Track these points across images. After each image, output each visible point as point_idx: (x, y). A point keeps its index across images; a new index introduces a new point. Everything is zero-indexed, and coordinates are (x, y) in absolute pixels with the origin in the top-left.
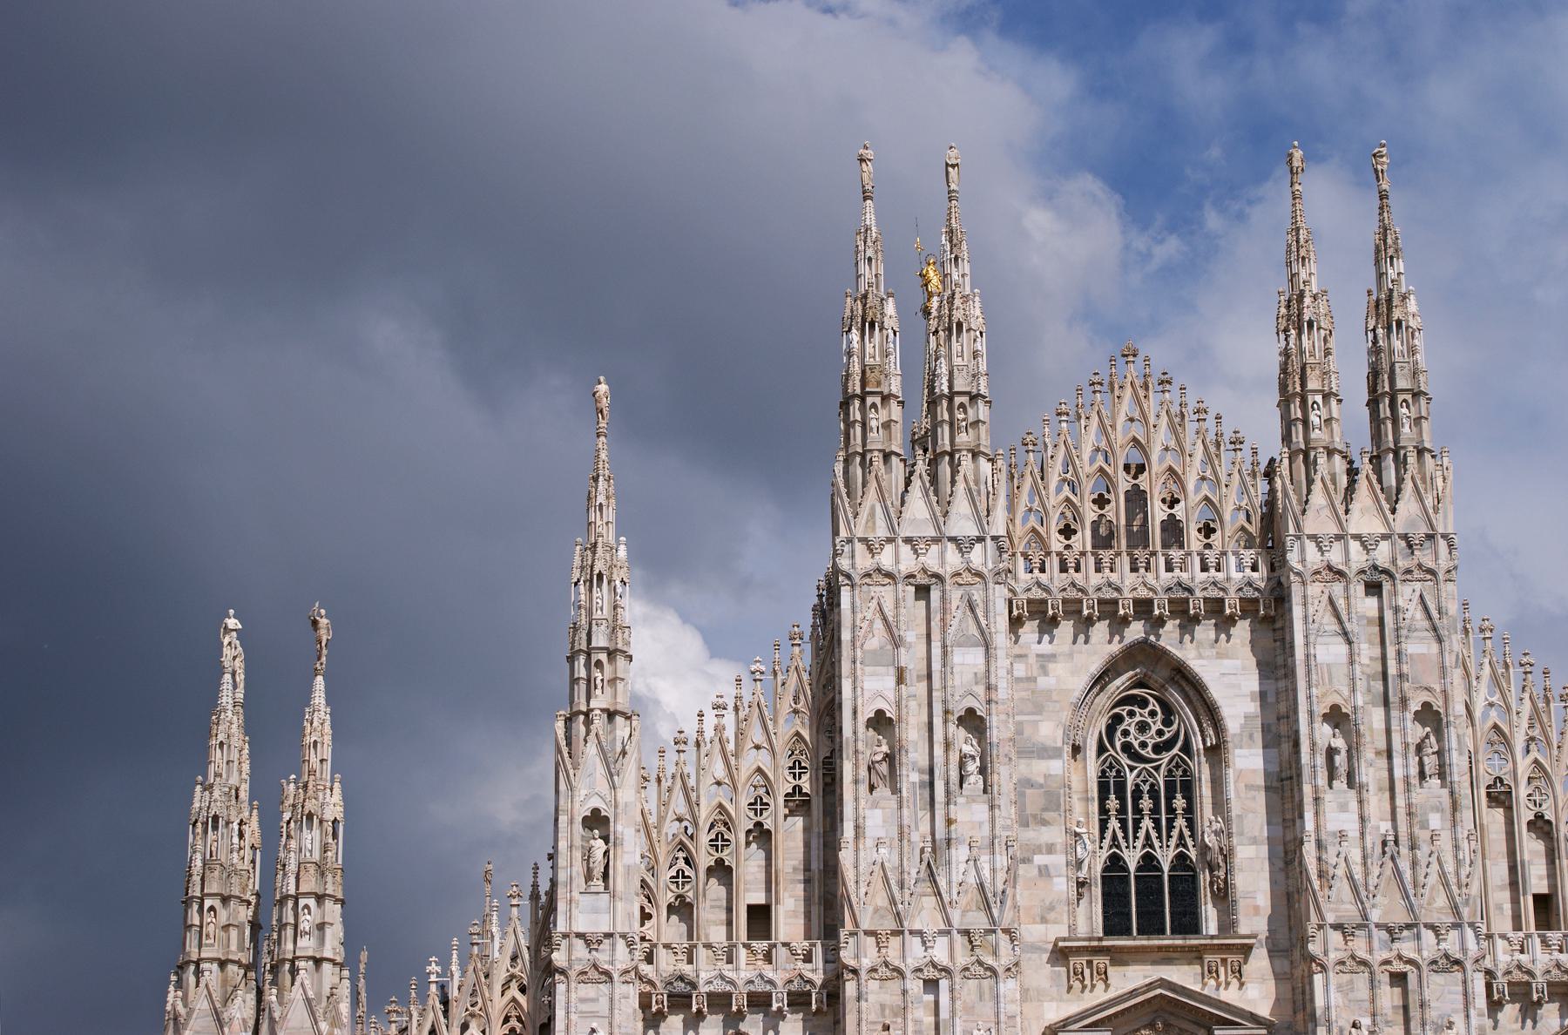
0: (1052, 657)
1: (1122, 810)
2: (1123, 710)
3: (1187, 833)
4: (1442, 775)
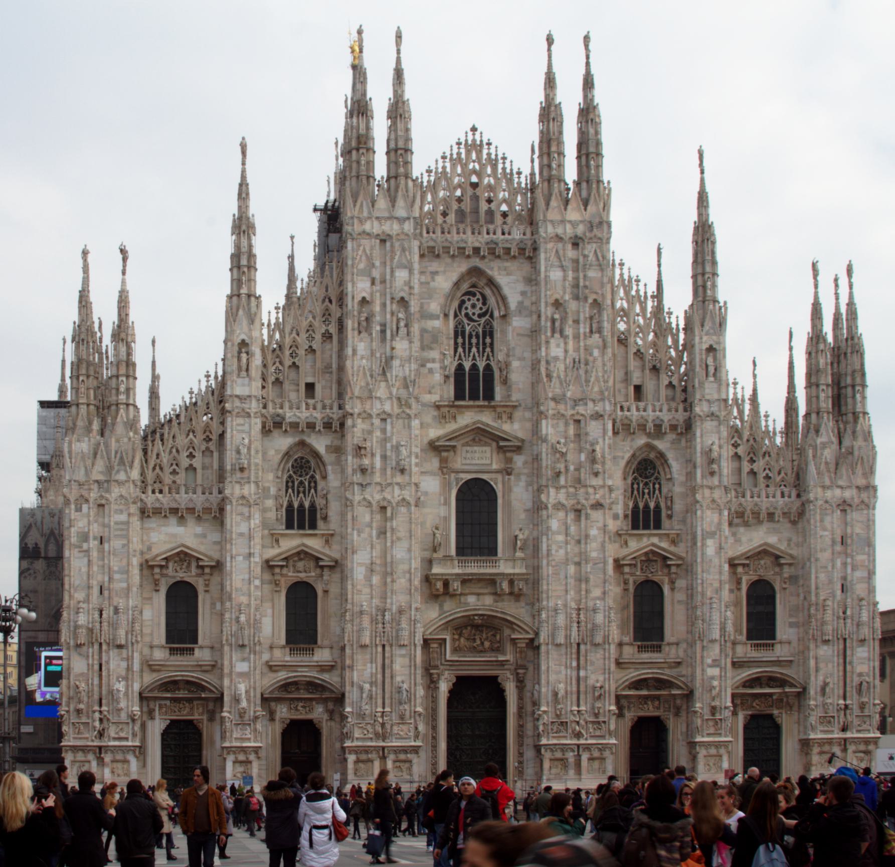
0: (436, 273)
1: (464, 344)
3: (491, 354)
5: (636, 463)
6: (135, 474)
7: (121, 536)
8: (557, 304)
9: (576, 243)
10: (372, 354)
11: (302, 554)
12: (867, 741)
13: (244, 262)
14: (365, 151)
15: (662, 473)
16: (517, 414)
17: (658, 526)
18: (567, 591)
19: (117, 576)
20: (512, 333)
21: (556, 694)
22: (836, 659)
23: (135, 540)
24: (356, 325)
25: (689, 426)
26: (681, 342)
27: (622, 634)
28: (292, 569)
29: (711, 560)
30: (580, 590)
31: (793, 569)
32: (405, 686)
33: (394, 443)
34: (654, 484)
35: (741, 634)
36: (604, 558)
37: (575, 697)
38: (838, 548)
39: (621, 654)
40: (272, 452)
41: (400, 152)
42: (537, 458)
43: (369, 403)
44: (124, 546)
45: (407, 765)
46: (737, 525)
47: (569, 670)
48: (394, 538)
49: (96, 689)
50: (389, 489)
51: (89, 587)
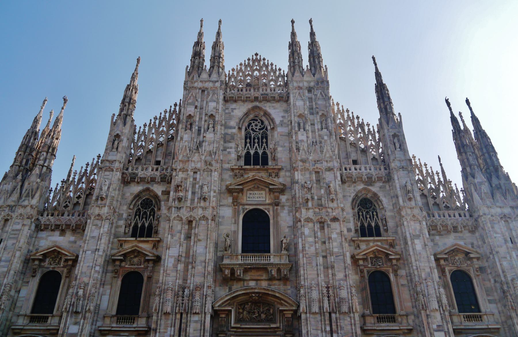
0: (235, 109)
1: (250, 143)
2: (252, 122)
3: (266, 147)
5: (359, 200)
7: (13, 238)
8: (300, 116)
9: (310, 90)
11: (136, 253)
13: (127, 100)
14: (198, 57)
15: (377, 206)
16: (282, 173)
18: (318, 275)
23: (22, 241)
24: (184, 127)
26: (377, 137)
27: (364, 308)
28: (128, 263)
29: (420, 253)
30: (328, 275)
31: (480, 263)
33: (200, 184)
34: (373, 213)
36: (343, 252)
38: (510, 245)
39: (365, 324)
40: (128, 194)
41: (217, 58)
42: (294, 197)
46: (433, 235)
47: (324, 333)
48: (196, 239)
50: (195, 210)
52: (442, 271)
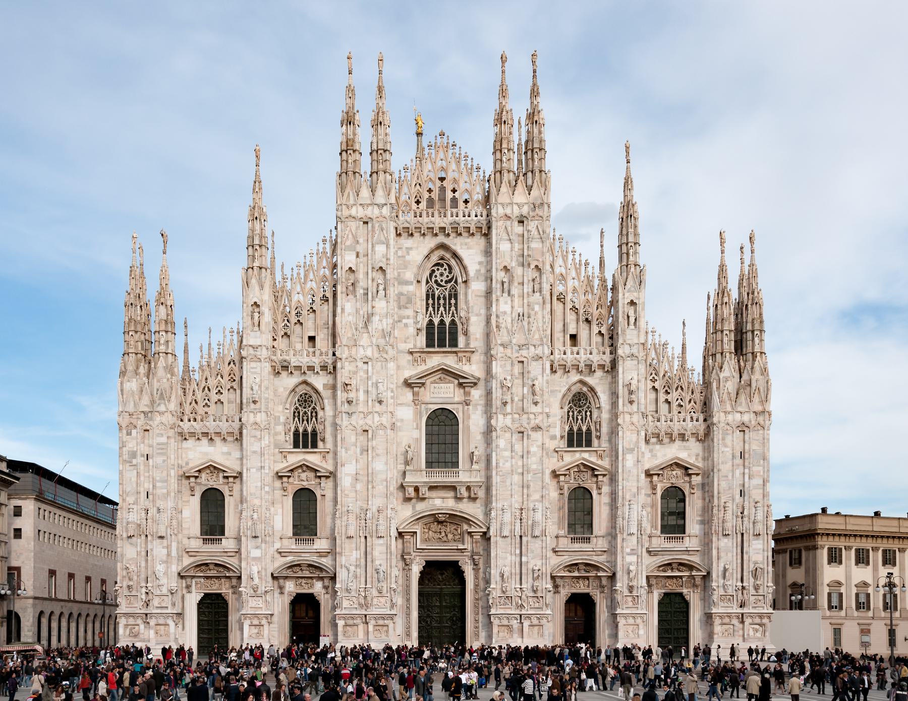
0: (411, 249)
1: (433, 304)
2: (435, 268)
4: (540, 292)
6: (173, 406)
10: (357, 311)
12: (761, 616)
15: (593, 403)
17: (589, 444)
19: (158, 484)
20: (472, 295)
21: (502, 576)
22: (735, 549)
23: (172, 456)
25: (614, 364)
32: (383, 568)
35: (656, 529)
37: (518, 577)
38: (738, 461)
39: (557, 546)
40: (281, 390)
42: (489, 393)
43: (354, 349)
44: (164, 461)
45: (385, 628)
49: (143, 570)
50: (370, 416)
51: (138, 493)
52: (654, 488)
